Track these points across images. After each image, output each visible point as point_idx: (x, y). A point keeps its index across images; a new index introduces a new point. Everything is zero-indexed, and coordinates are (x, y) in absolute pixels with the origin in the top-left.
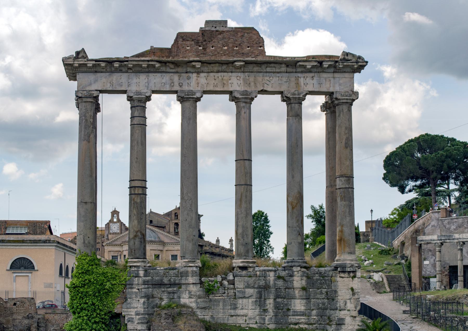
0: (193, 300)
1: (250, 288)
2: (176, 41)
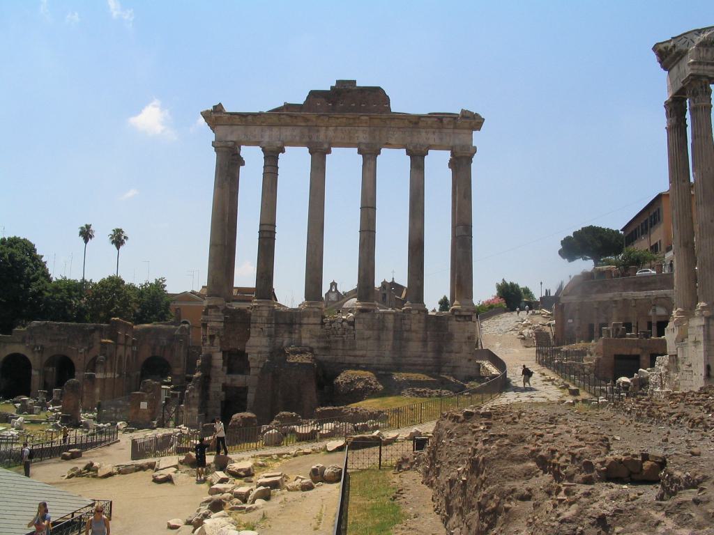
0: (314, 340)
1: (370, 329)
2: (308, 97)
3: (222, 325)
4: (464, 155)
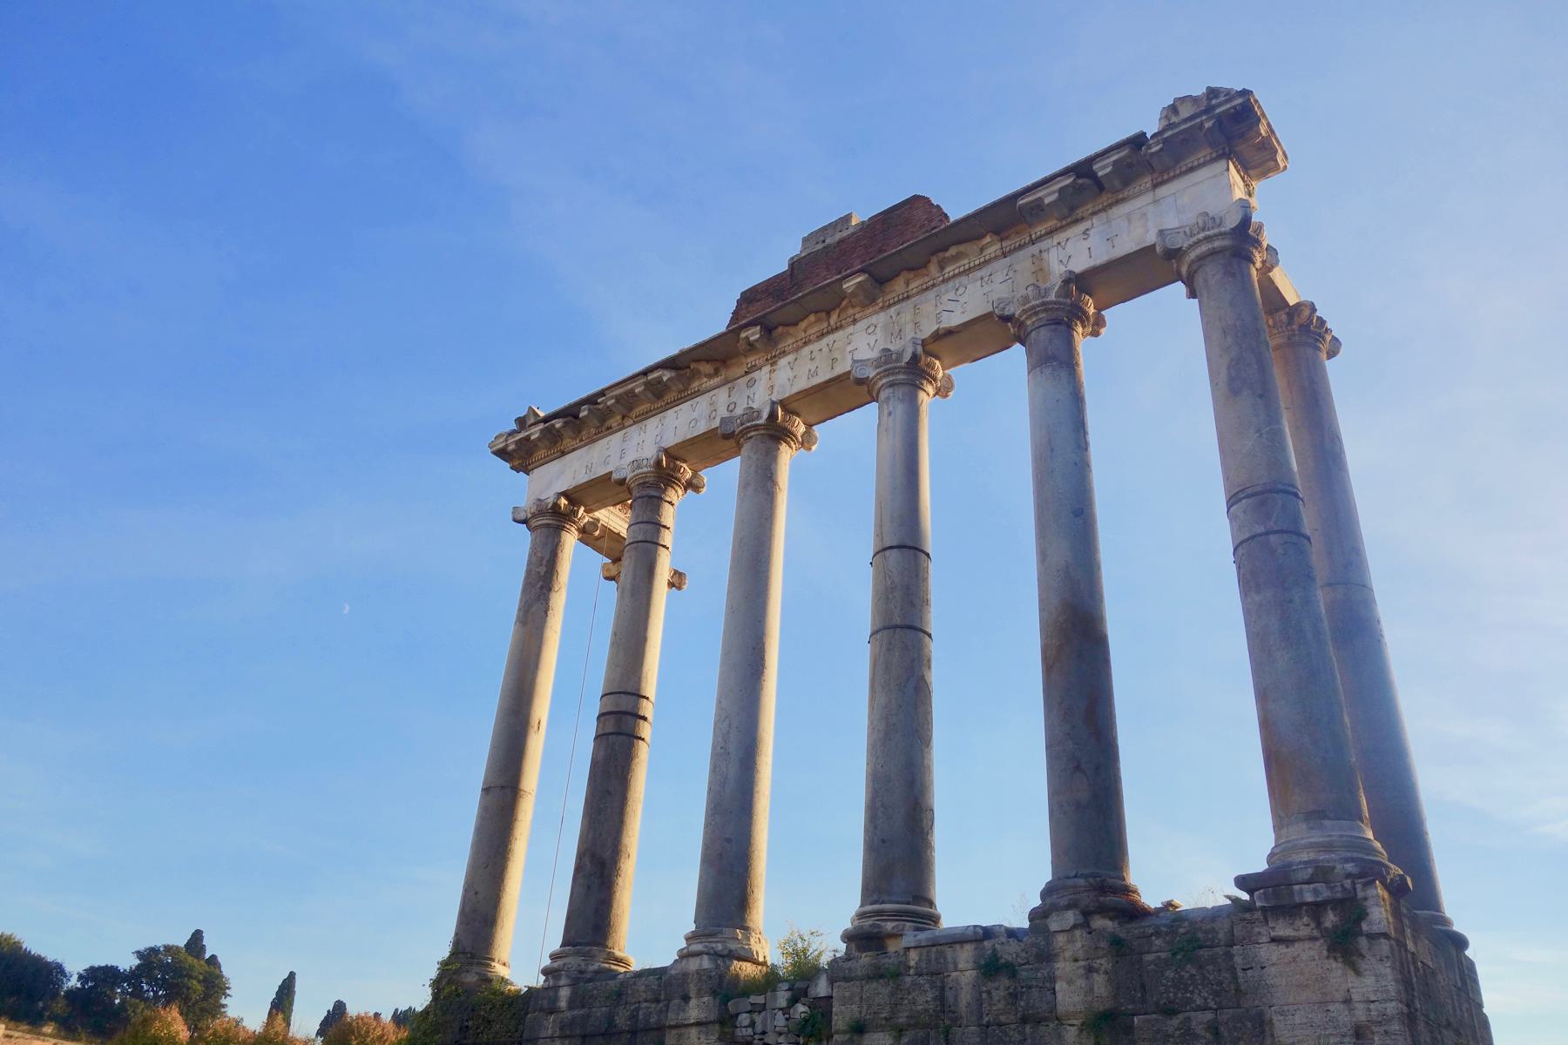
4: (1204, 248)
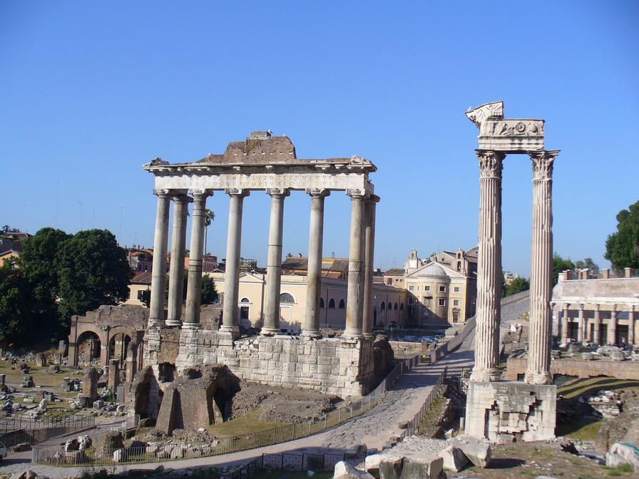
3: (159, 342)
